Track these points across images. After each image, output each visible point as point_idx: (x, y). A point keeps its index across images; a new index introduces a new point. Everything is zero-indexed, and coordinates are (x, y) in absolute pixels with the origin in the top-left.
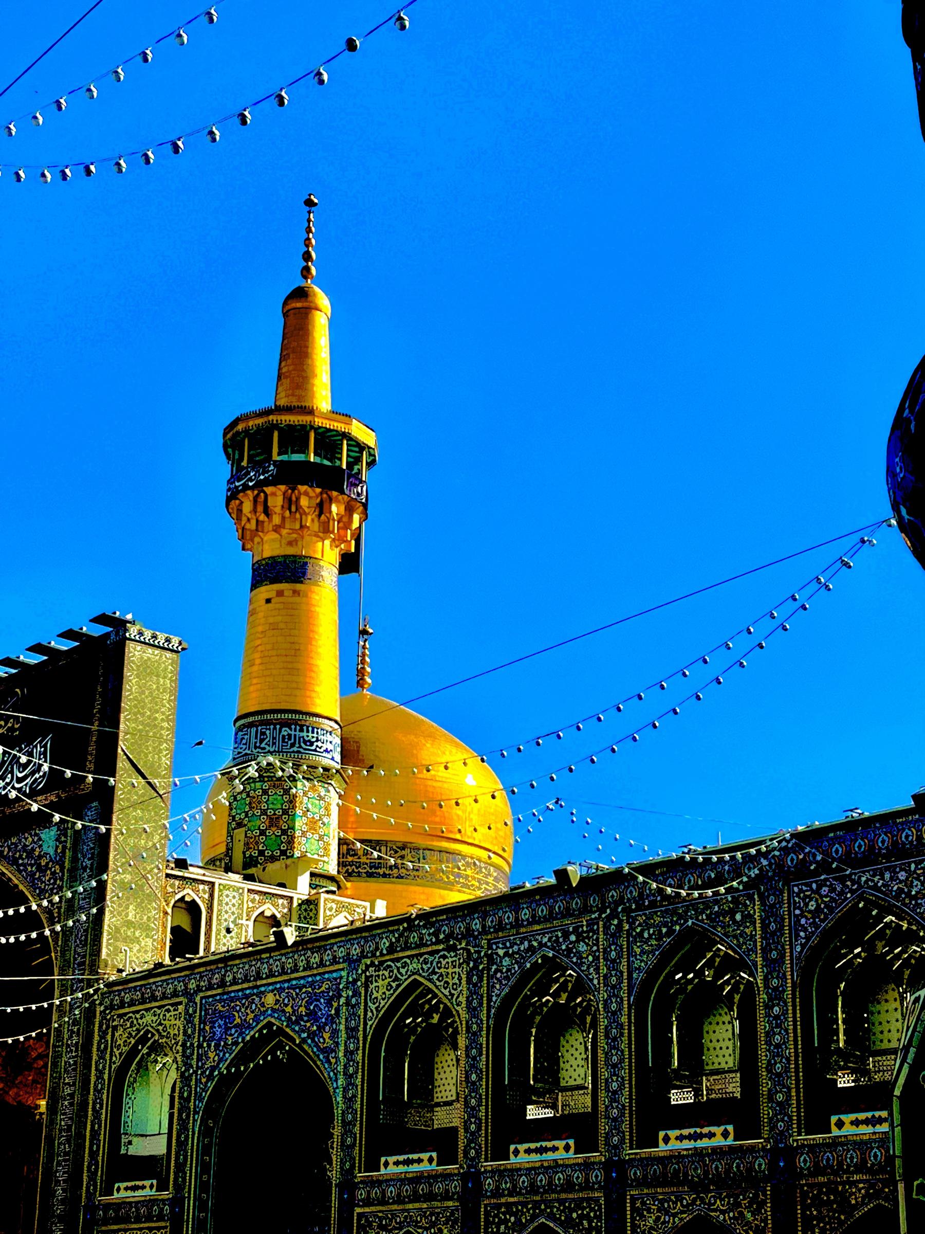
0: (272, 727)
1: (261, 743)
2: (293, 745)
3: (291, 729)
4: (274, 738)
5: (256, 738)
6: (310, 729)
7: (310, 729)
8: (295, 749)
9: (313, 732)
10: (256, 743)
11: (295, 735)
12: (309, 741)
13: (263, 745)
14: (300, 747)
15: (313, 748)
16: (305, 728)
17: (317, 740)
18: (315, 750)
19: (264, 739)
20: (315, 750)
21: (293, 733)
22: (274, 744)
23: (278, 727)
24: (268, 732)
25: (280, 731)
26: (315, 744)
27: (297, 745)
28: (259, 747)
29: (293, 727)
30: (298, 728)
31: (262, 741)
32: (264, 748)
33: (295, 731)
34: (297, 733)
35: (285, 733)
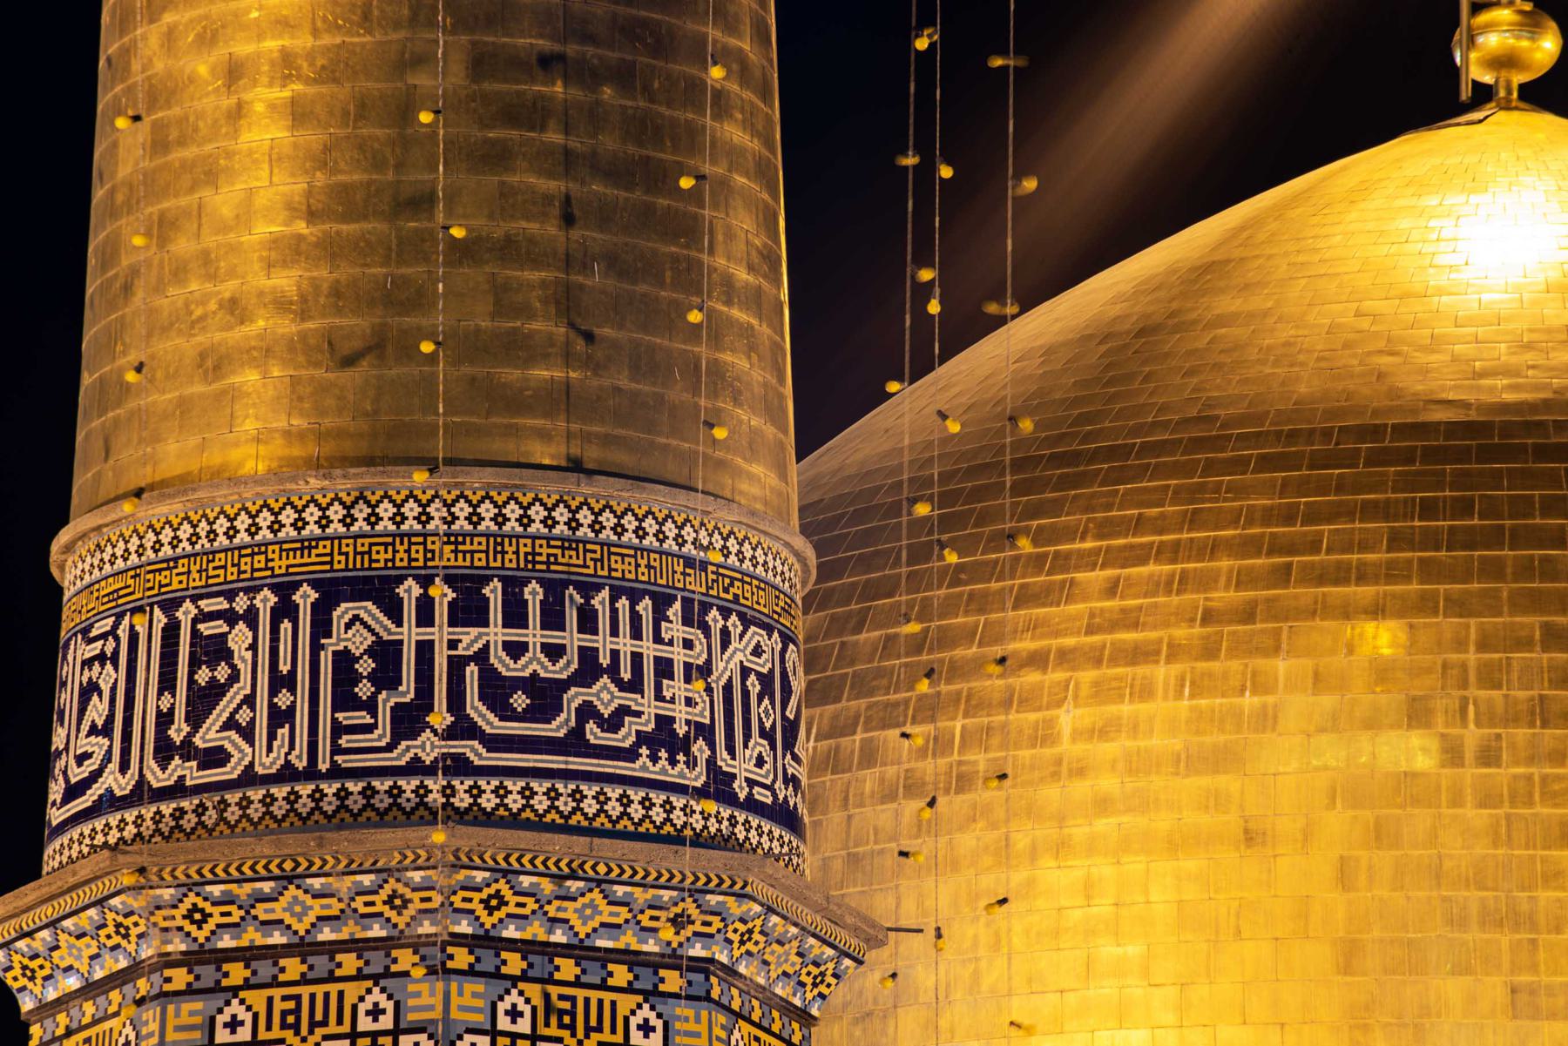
0: (266, 601)
1: (196, 718)
2: (409, 721)
3: (394, 611)
4: (283, 681)
5: (167, 683)
6: (533, 594)
7: (533, 594)
8: (428, 747)
9: (553, 619)
10: (165, 719)
11: (425, 650)
12: (532, 684)
13: (209, 735)
14: (463, 728)
15: (557, 728)
16: (494, 592)
17: (589, 669)
18: (575, 743)
19: (216, 691)
20: (575, 743)
21: (409, 634)
22: (280, 717)
23: (305, 597)
24: (239, 639)
25: (322, 627)
26: (574, 697)
27: (440, 718)
28: (187, 750)
29: (409, 591)
30: (442, 594)
31: (203, 701)
32: (215, 757)
33: (425, 616)
34: (440, 633)
35: (358, 641)
